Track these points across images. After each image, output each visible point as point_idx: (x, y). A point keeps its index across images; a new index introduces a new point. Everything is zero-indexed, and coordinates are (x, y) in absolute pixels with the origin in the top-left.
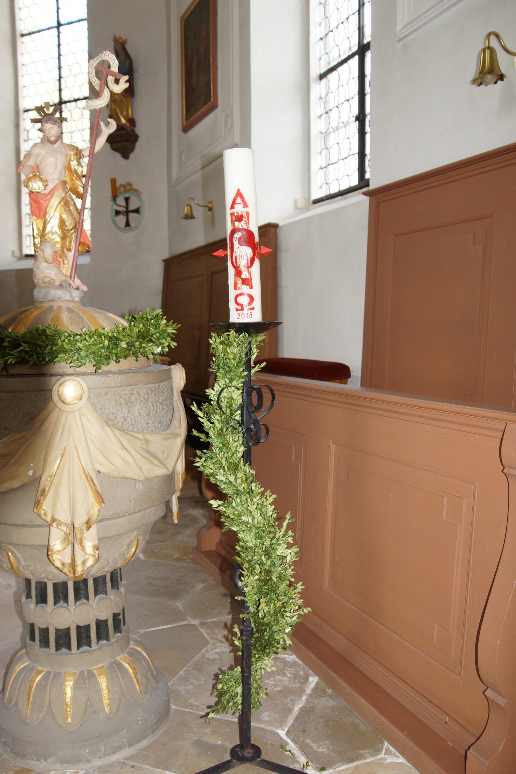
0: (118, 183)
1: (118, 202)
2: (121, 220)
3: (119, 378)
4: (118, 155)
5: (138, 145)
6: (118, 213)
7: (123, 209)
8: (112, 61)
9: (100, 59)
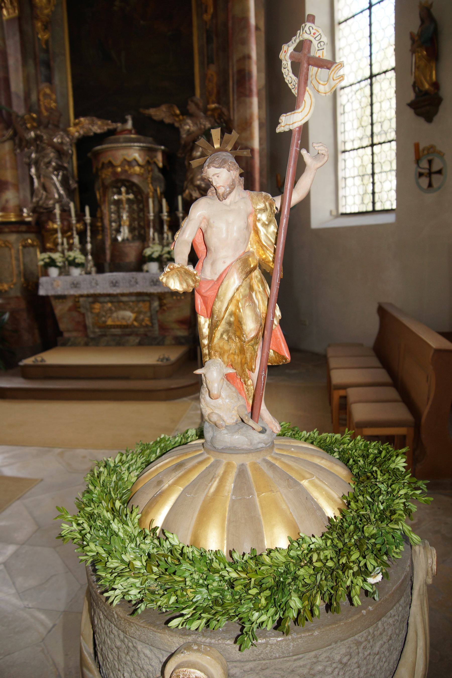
0: (421, 147)
1: (421, 165)
2: (424, 181)
3: (292, 644)
6: (421, 175)
7: (426, 171)
8: (317, 39)
9: (298, 41)
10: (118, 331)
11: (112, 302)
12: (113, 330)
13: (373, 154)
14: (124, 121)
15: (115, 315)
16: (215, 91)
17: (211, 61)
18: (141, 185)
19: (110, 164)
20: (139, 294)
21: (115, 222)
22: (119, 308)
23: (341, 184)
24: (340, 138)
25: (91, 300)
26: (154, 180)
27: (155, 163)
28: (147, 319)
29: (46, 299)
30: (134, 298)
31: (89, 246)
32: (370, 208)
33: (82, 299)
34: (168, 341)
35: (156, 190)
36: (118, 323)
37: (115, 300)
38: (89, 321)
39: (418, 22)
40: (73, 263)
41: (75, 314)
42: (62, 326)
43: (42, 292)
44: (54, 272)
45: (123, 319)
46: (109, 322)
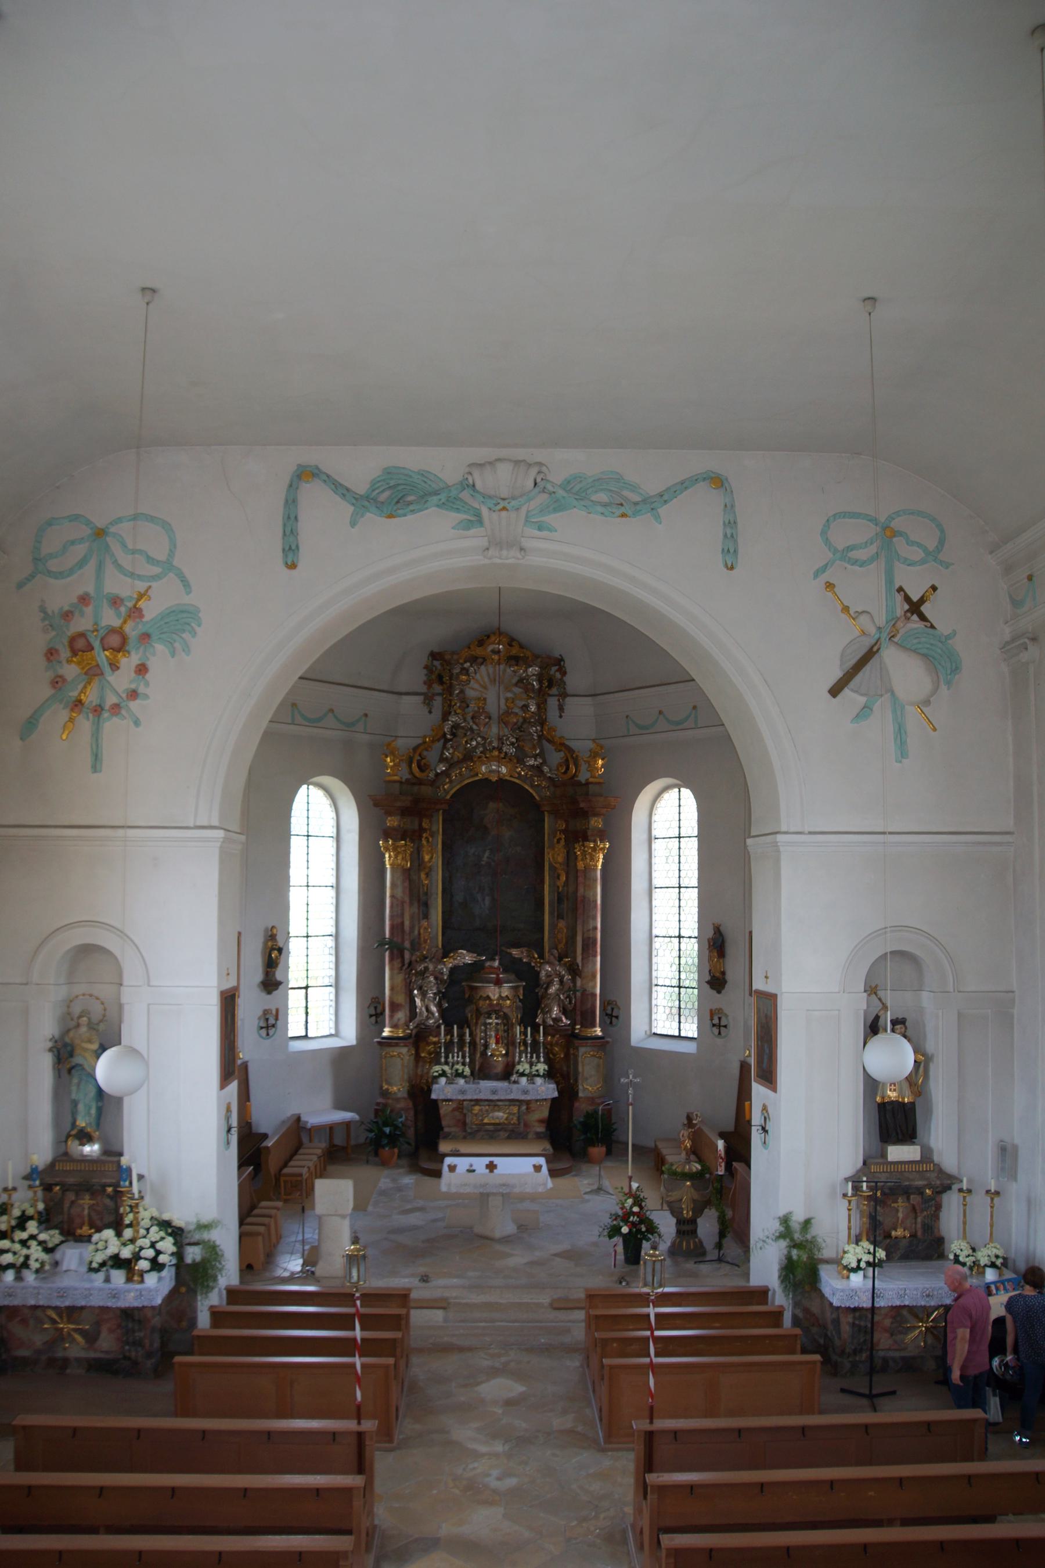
2: (716, 1030)
4: (714, 992)
5: (726, 986)
6: (714, 1025)
10: (491, 1128)
11: (489, 1105)
12: (487, 1127)
13: (679, 993)
14: (494, 960)
15: (491, 1115)
16: (564, 941)
17: (560, 916)
18: (510, 1014)
19: (488, 998)
20: (510, 1100)
21: (483, 1039)
22: (493, 1111)
23: (654, 1010)
24: (654, 974)
25: (473, 1103)
26: (517, 1008)
27: (519, 997)
28: (515, 1118)
29: (436, 1101)
30: (507, 1103)
31: (468, 1060)
32: (677, 1034)
33: (465, 1103)
34: (530, 1136)
35: (517, 1016)
36: (493, 1122)
37: (493, 1103)
38: (468, 1121)
39: (713, 932)
40: (459, 1075)
41: (457, 1113)
42: (444, 1123)
43: (434, 1096)
44: (443, 1080)
45: (497, 1118)
46: (486, 1121)
